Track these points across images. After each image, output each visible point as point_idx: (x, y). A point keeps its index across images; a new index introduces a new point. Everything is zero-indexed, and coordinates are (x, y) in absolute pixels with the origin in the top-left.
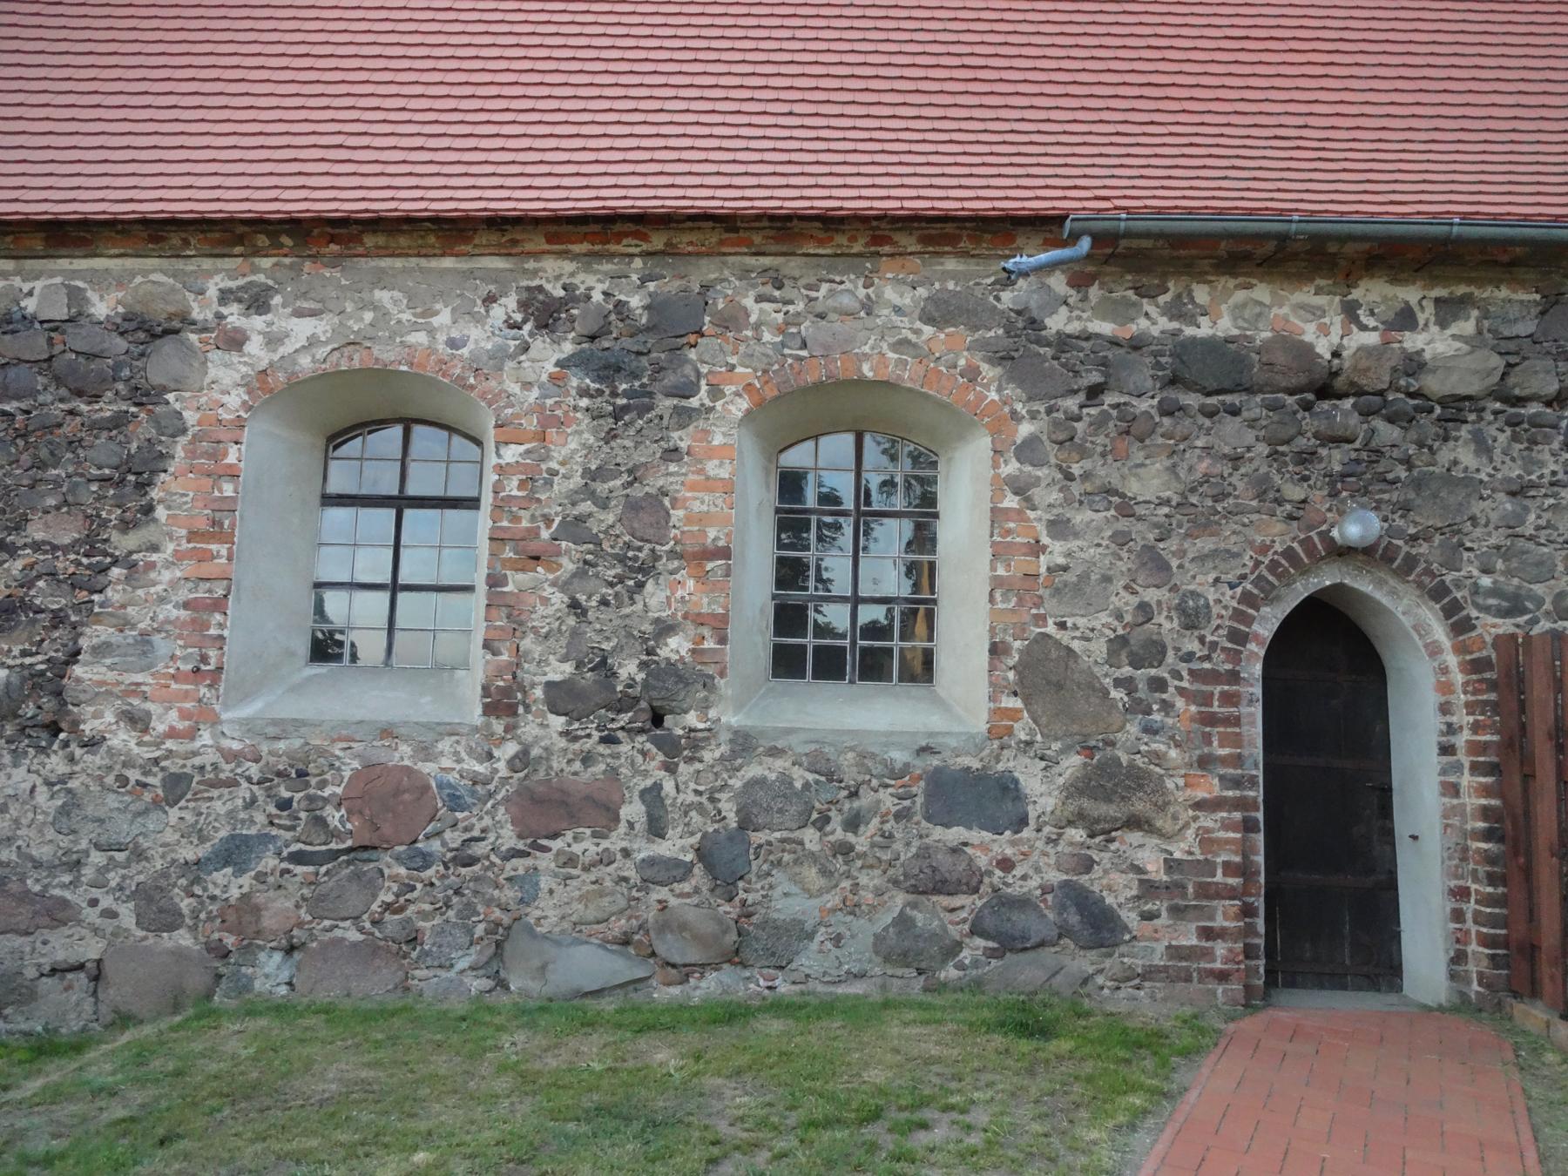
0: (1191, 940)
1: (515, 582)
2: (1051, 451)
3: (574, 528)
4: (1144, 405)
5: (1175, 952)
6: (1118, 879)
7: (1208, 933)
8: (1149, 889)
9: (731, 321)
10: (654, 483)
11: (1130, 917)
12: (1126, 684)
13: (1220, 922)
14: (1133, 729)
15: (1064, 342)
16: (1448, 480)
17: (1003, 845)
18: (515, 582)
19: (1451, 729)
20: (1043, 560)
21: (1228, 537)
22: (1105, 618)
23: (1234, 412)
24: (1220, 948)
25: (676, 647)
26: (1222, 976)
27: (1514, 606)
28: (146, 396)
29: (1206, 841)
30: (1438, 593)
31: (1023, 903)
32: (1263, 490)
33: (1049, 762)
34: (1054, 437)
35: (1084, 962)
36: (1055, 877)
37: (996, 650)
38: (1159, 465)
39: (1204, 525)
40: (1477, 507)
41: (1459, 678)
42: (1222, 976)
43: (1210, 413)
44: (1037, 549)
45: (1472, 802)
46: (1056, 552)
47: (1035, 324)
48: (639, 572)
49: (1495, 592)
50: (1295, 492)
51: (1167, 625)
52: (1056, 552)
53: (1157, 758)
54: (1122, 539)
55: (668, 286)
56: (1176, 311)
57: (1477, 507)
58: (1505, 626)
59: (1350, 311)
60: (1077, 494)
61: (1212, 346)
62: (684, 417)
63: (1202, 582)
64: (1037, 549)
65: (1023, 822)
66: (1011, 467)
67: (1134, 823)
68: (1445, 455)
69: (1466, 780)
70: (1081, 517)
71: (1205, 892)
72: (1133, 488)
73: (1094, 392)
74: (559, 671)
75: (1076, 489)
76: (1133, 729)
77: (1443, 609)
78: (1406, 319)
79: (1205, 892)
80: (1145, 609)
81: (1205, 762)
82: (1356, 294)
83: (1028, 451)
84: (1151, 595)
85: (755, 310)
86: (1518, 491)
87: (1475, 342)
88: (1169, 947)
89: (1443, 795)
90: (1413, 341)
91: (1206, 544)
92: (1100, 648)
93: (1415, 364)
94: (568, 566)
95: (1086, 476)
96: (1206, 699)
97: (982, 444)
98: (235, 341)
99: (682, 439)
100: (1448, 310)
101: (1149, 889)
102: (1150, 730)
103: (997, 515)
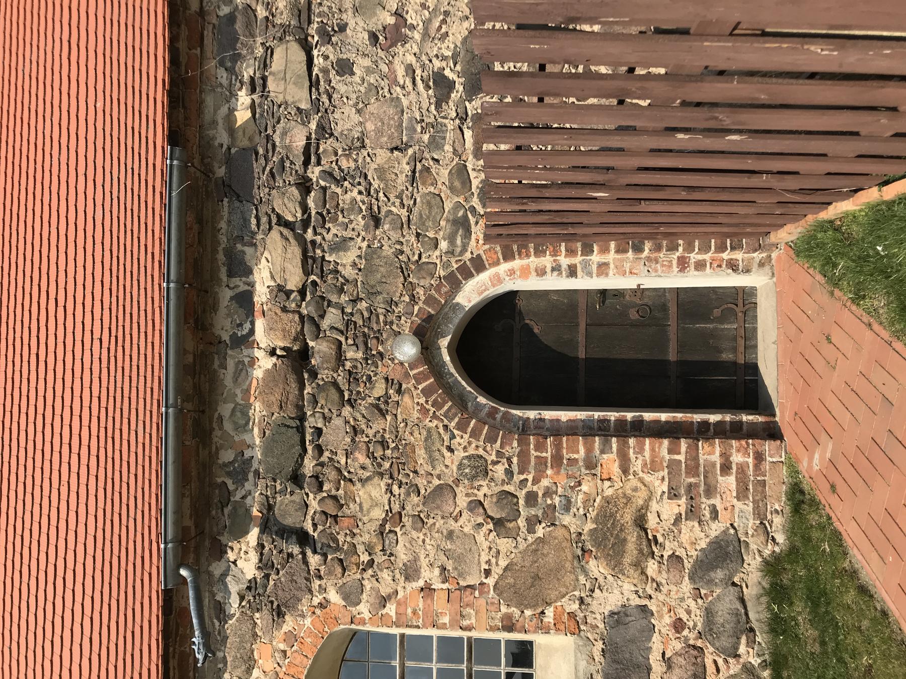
0: (730, 482)
2: (353, 575)
4: (314, 504)
5: (742, 494)
6: (685, 537)
7: (726, 468)
8: (693, 512)
11: (716, 529)
12: (532, 523)
13: (716, 458)
14: (567, 519)
15: (265, 565)
16: (368, 271)
17: (663, 623)
19: (556, 268)
20: (437, 585)
21: (416, 439)
22: (480, 538)
23: (319, 432)
24: (737, 458)
26: (759, 457)
27: (462, 225)
29: (653, 466)
30: (454, 283)
31: (709, 614)
32: (380, 409)
33: (595, 586)
34: (340, 575)
35: (753, 564)
36: (687, 586)
38: (361, 493)
39: (405, 455)
40: (388, 251)
41: (517, 263)
42: (759, 457)
43: (320, 450)
44: (427, 590)
45: (611, 256)
49: (451, 239)
50: (379, 389)
51: (485, 490)
53: (588, 501)
54: (420, 521)
57: (388, 251)
58: (478, 230)
60: (384, 558)
63: (451, 464)
64: (427, 590)
65: (644, 609)
67: (640, 523)
68: (348, 272)
69: (596, 258)
70: (402, 555)
71: (693, 469)
72: (378, 514)
75: (379, 558)
76: (567, 519)
77: (465, 279)
79: (693, 469)
80: (476, 505)
81: (591, 464)
82: (226, 337)
84: (462, 501)
88: (738, 498)
89: (607, 275)
91: (421, 453)
92: (505, 544)
95: (370, 550)
96: (542, 462)
101: (693, 512)
102: (567, 506)
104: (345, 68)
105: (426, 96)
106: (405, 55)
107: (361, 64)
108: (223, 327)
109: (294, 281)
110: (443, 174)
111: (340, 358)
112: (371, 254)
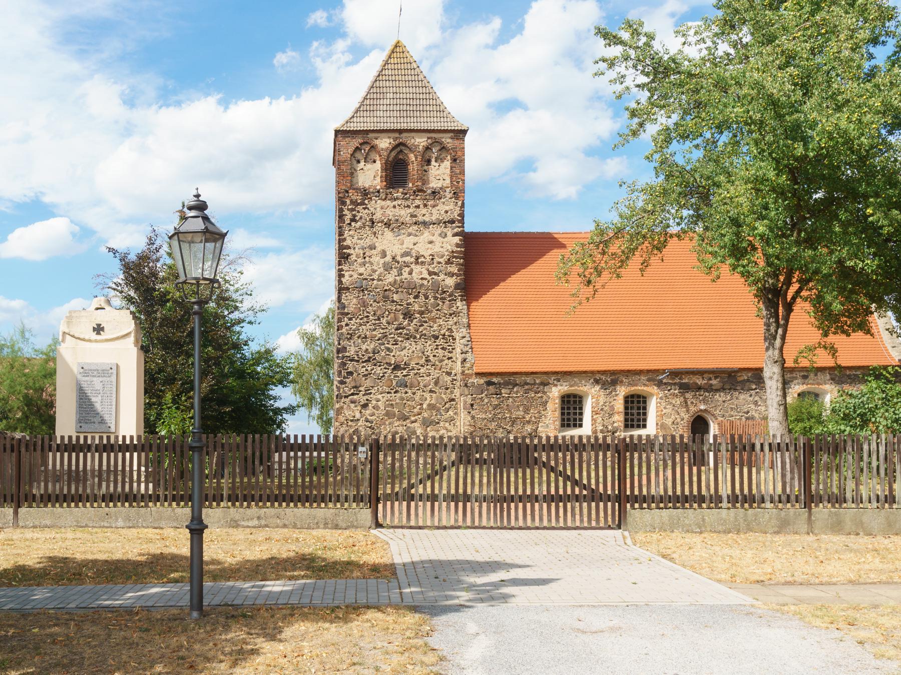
1: (595, 417)
3: (602, 409)
9: (622, 382)
10: (612, 404)
18: (595, 417)
25: (615, 425)
28: (545, 393)
37: (657, 424)
46: (665, 411)
47: (662, 381)
48: (611, 416)
52: (665, 411)
55: (613, 377)
56: (680, 379)
59: (703, 378)
61: (685, 383)
62: (617, 395)
63: (683, 414)
64: (662, 411)
66: (659, 400)
73: (669, 390)
74: (601, 428)
78: (710, 379)
83: (661, 398)
85: (624, 380)
86: (724, 402)
87: (720, 381)
90: (711, 382)
93: (711, 385)
94: (601, 415)
97: (655, 398)
98: (556, 385)
99: (615, 398)
100: (716, 378)
103: (657, 407)
104: (751, 396)
105: (746, 410)
106: (753, 406)
107: (751, 399)
108: (705, 376)
109: (713, 388)
110: (732, 413)
111: (700, 395)
112: (718, 401)
